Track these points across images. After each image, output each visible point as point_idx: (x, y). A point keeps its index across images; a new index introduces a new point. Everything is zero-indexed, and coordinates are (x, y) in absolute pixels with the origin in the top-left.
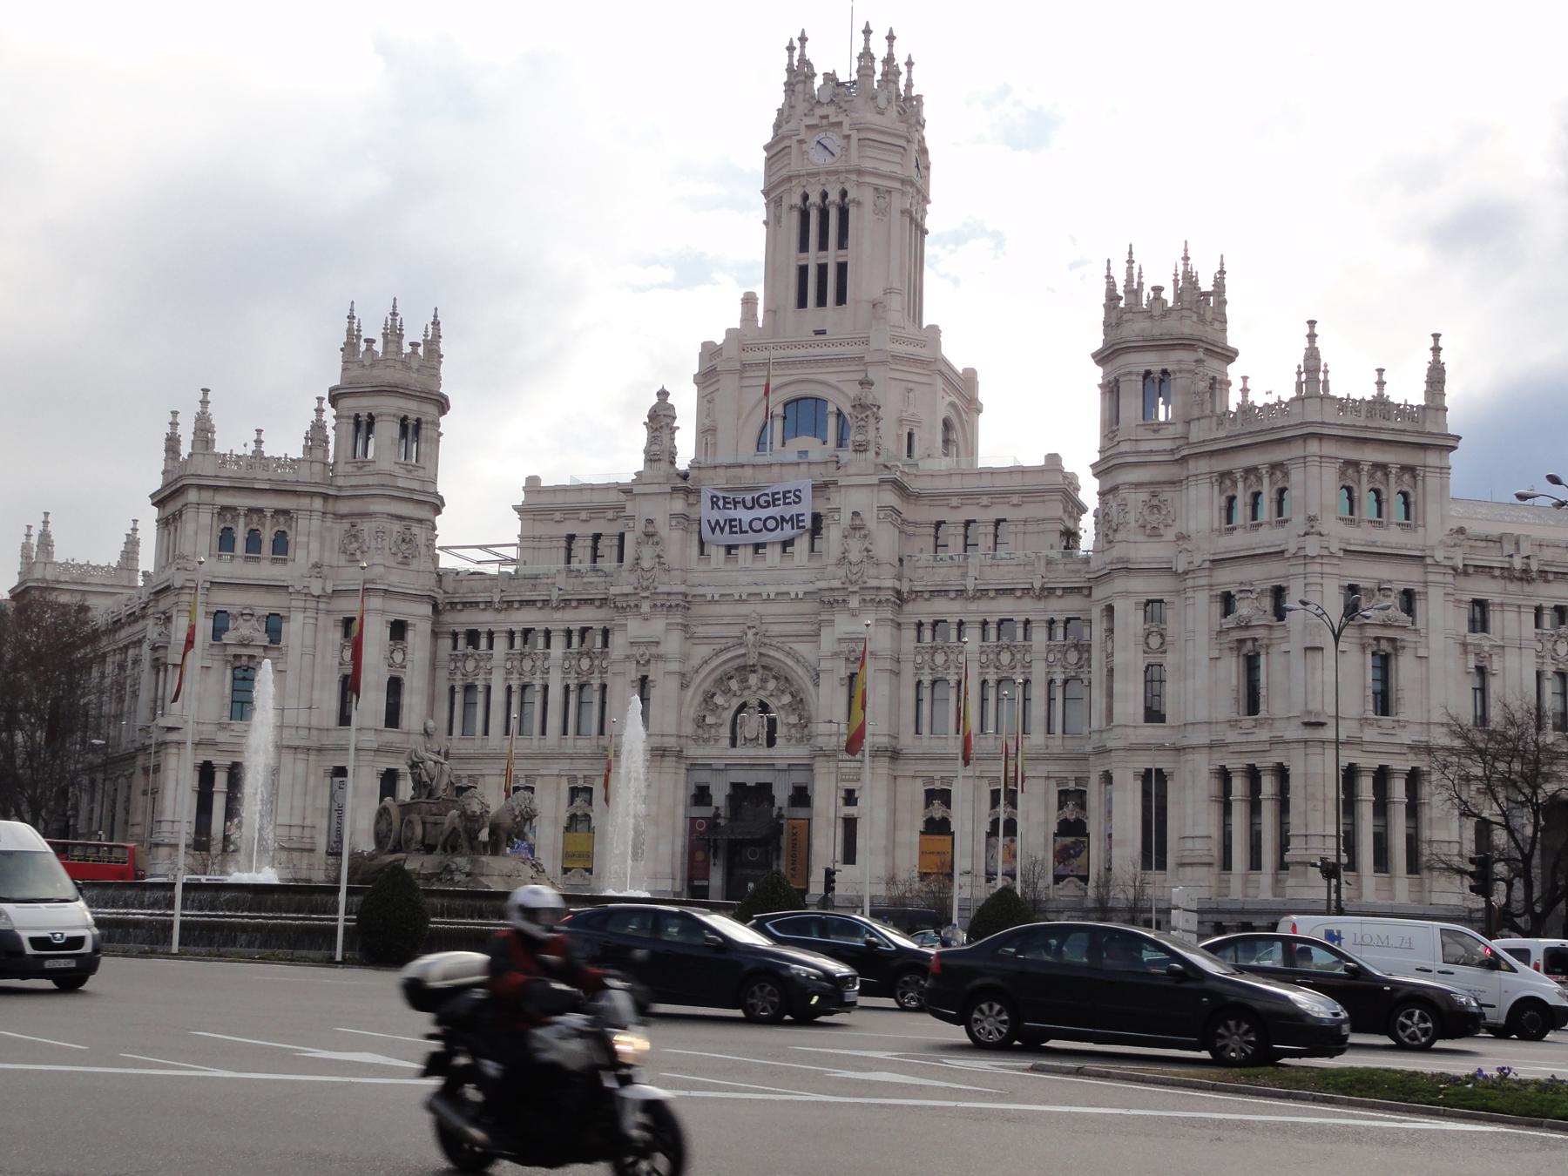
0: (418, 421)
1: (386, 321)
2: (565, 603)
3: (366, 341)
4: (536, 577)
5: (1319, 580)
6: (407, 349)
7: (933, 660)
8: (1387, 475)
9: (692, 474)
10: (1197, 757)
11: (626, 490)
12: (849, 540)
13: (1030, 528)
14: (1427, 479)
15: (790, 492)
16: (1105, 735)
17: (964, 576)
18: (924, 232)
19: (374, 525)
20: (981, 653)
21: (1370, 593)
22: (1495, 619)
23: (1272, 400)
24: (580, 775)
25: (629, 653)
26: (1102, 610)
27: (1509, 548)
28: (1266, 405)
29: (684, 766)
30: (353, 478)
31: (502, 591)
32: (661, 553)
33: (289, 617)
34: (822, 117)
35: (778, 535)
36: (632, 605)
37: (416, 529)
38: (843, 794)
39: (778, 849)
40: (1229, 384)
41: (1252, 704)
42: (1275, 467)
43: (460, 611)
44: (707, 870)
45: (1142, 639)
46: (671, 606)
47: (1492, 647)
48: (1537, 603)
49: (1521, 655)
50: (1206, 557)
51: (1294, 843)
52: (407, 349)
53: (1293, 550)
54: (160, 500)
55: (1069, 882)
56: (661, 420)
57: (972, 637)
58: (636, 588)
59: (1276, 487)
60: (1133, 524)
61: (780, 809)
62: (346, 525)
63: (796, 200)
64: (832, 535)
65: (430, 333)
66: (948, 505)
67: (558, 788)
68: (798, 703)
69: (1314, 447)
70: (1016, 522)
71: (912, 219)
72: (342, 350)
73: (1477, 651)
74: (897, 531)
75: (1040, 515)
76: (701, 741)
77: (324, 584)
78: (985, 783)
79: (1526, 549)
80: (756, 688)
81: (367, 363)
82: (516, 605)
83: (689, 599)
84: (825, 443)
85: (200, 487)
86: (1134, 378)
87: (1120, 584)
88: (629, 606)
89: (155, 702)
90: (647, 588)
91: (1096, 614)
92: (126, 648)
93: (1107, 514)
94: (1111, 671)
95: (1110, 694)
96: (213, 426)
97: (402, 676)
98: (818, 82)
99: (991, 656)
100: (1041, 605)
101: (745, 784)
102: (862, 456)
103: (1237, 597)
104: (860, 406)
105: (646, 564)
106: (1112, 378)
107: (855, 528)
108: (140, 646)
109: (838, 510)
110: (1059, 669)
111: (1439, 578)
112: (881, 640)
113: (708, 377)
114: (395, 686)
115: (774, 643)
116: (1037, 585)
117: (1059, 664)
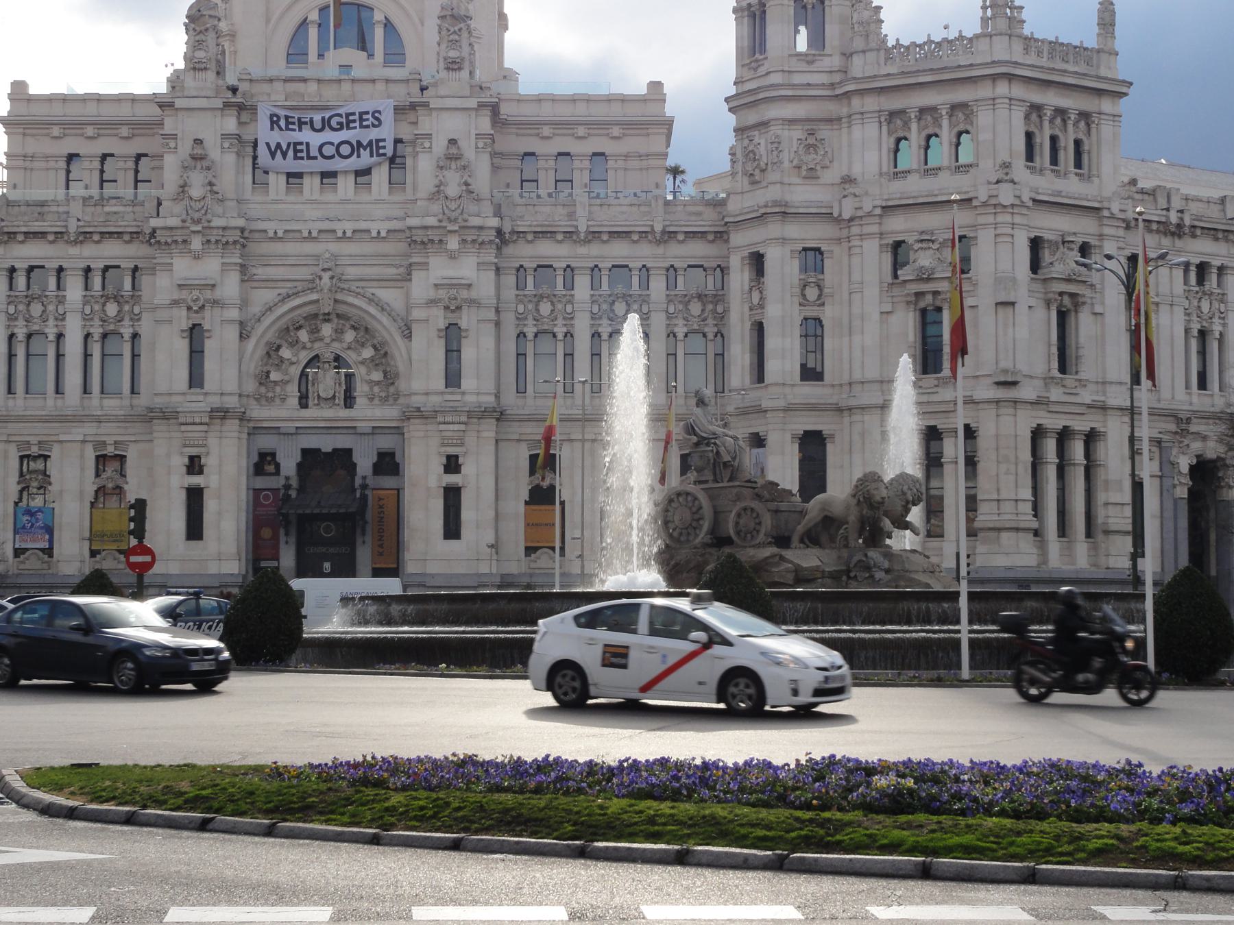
2: (85, 237)
4: (43, 204)
5: (1009, 231)
7: (538, 310)
10: (866, 418)
11: (164, 104)
12: (445, 173)
15: (367, 113)
17: (571, 215)
21: (1054, 245)
24: (34, 440)
25: (176, 297)
26: (743, 258)
27: (1162, 203)
28: (945, 40)
32: (214, 180)
35: (354, 163)
36: (180, 240)
38: (444, 460)
42: (954, 108)
44: (276, 548)
45: (798, 290)
46: (227, 243)
49: (1172, 313)
50: (878, 203)
51: (983, 508)
58: (184, 221)
60: (786, 164)
64: (423, 168)
66: (573, 135)
67: (82, 456)
68: (382, 356)
69: (1002, 88)
76: (264, 402)
79: (1177, 203)
80: (328, 339)
82: (20, 237)
83: (246, 234)
84: (371, 56)
87: (774, 229)
88: (176, 242)
90: (199, 221)
91: (735, 261)
99: (605, 306)
100: (660, 250)
101: (319, 450)
102: (455, 75)
105: (196, 192)
107: (450, 158)
109: (428, 136)
112: (485, 287)
115: (353, 288)
116: (658, 228)
117: (680, 316)
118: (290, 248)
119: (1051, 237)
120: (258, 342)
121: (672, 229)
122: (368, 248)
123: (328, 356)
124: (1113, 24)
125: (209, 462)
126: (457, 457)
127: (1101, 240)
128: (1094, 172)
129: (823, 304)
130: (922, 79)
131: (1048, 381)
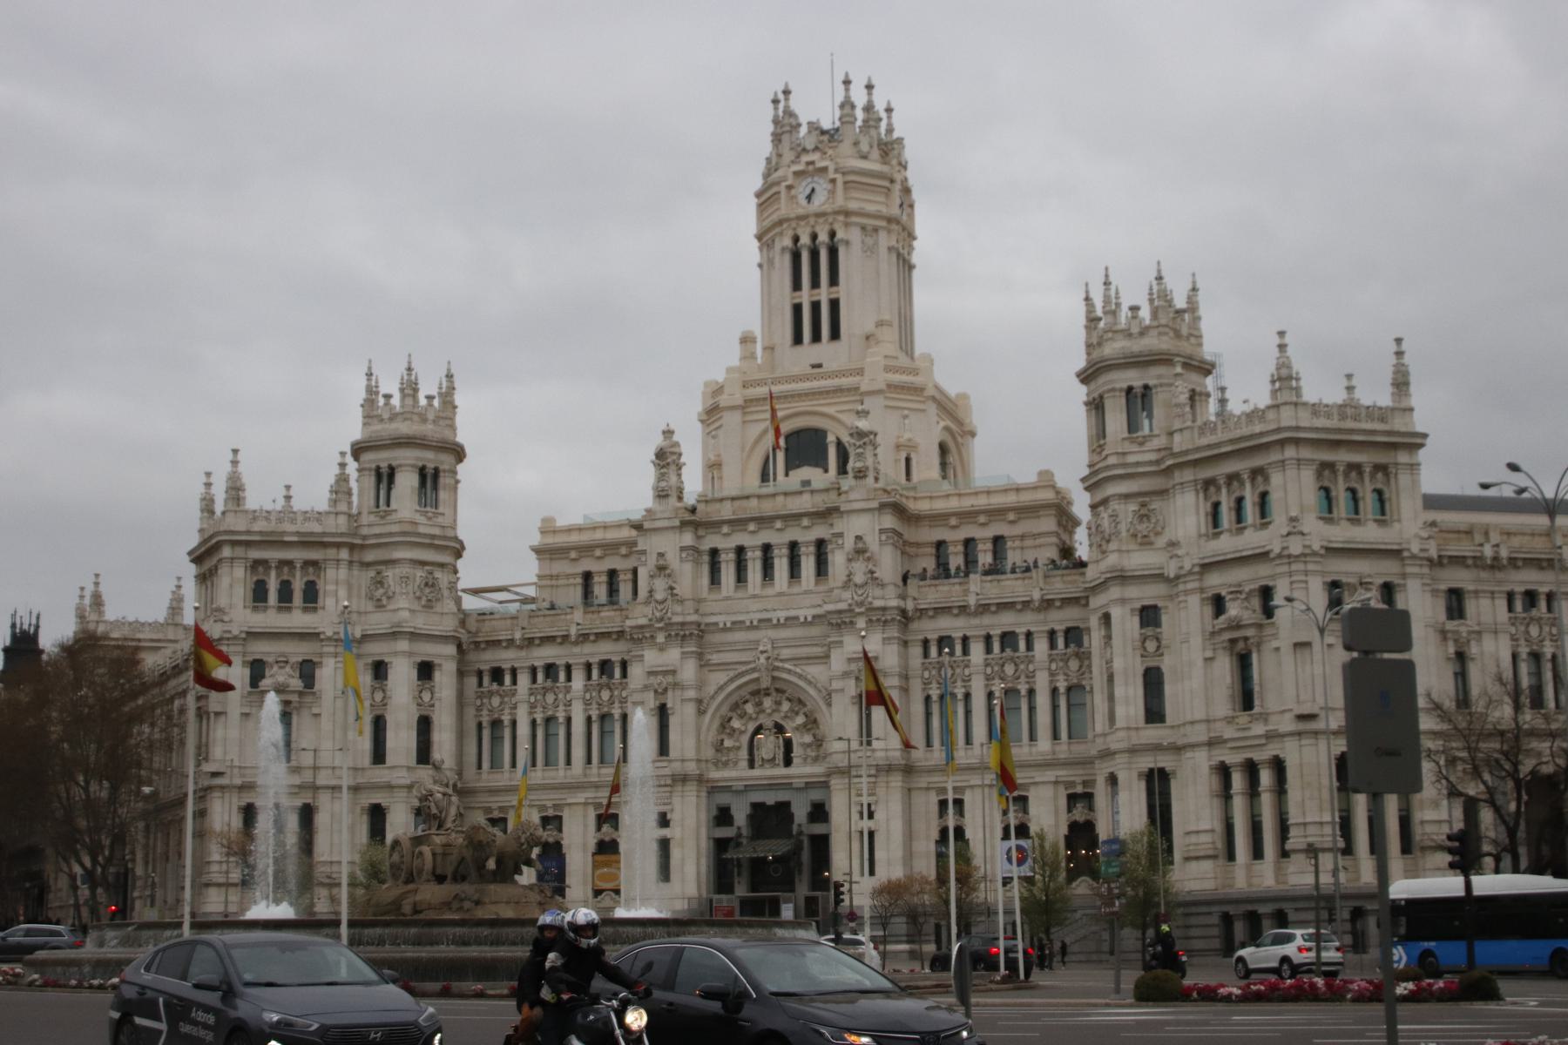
2: (584, 638)
5: (1303, 578)
6: (423, 402)
9: (701, 507)
11: (638, 526)
12: (853, 564)
13: (1028, 543)
16: (1109, 738)
18: (911, 267)
19: (397, 571)
20: (987, 665)
22: (1471, 606)
23: (1248, 408)
26: (1100, 619)
27: (1478, 538)
28: (1243, 413)
29: (705, 789)
31: (523, 628)
32: (674, 585)
33: (321, 663)
36: (648, 635)
37: (438, 574)
39: (800, 864)
41: (1247, 700)
43: (484, 649)
45: (1140, 644)
46: (684, 636)
47: (1470, 633)
48: (1508, 588)
50: (1196, 561)
51: (1293, 832)
52: (423, 402)
53: (1277, 550)
55: (1083, 881)
56: (667, 458)
57: (977, 651)
58: (650, 620)
59: (1258, 491)
60: (1124, 534)
61: (800, 825)
62: (372, 573)
64: (837, 560)
65: (444, 385)
67: (585, 816)
68: (812, 723)
69: (1290, 452)
70: (1013, 538)
71: (899, 255)
73: (1456, 637)
74: (899, 552)
75: (1035, 531)
79: (1495, 537)
81: (386, 416)
83: (702, 627)
84: (826, 471)
85: (234, 543)
86: (1118, 394)
87: (1115, 592)
91: (1094, 621)
94: (1111, 678)
95: (1111, 698)
96: (242, 485)
97: (431, 714)
98: (803, 130)
99: (996, 668)
100: (1041, 616)
102: (863, 482)
104: (860, 434)
105: (659, 596)
106: (1096, 395)
108: (185, 696)
109: (840, 535)
110: (1061, 677)
111: (1416, 570)
113: (712, 414)
114: (424, 725)
115: (787, 666)
116: (1036, 595)
117: (1061, 672)
118: (739, 636)
120: (713, 715)
122: (798, 632)
123: (768, 723)
124: (1407, 384)
125: (674, 817)
127: (1404, 579)
128: (1395, 517)
129: (1162, 655)
130: (1224, 450)
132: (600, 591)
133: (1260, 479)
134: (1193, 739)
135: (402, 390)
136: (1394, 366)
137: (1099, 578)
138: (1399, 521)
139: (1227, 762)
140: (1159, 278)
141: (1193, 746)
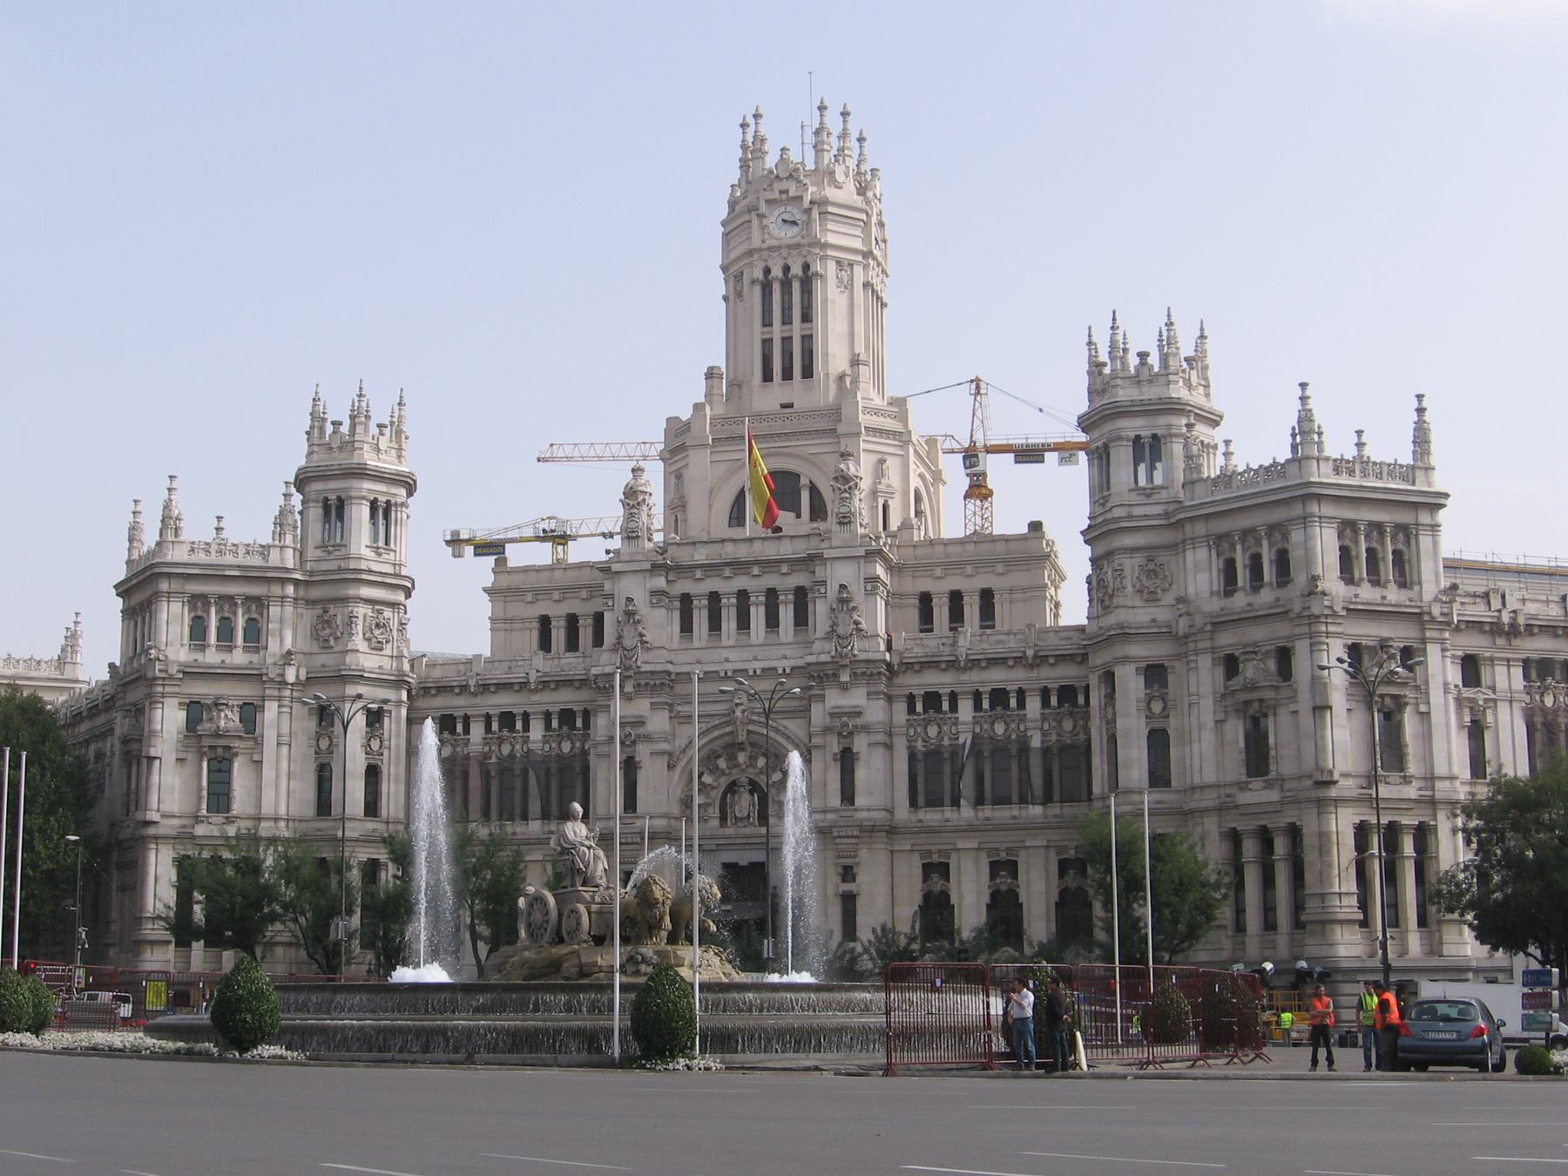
0: (388, 502)
1: (353, 403)
2: (544, 685)
3: (333, 423)
6: (374, 430)
8: (1382, 533)
11: (605, 569)
14: (1421, 537)
19: (346, 609)
21: (1370, 649)
26: (1099, 677)
27: (1496, 603)
30: (323, 563)
31: (478, 674)
32: (644, 632)
34: (781, 192)
37: (388, 613)
38: (840, 870)
40: (1215, 447)
42: (1272, 528)
43: (435, 695)
45: (1143, 704)
46: (655, 685)
47: (1486, 700)
50: (1208, 620)
53: (1297, 608)
54: (124, 590)
56: (633, 497)
59: (1275, 548)
60: (1130, 589)
62: (318, 611)
63: (759, 274)
64: (820, 611)
65: (396, 415)
69: (1314, 508)
72: (308, 433)
73: (1472, 705)
77: (298, 671)
78: (983, 855)
83: (673, 677)
84: (799, 516)
86: (1125, 443)
89: (128, 796)
91: (1093, 680)
92: (87, 742)
93: (1102, 579)
94: (1113, 740)
100: (1035, 674)
101: (737, 864)
103: (1241, 659)
105: (628, 643)
106: (1100, 444)
111: (1435, 634)
112: (875, 712)
114: (373, 774)
116: (1030, 653)
119: (1370, 643)
121: (1042, 654)
126: (851, 867)
129: (1168, 716)
131: (1373, 779)
132: (558, 636)
133: (1277, 535)
134: (1204, 804)
135: (352, 418)
136: (1415, 423)
137: (1103, 634)
138: (1420, 583)
139: (1238, 829)
140: (1169, 324)
141: (1203, 812)
